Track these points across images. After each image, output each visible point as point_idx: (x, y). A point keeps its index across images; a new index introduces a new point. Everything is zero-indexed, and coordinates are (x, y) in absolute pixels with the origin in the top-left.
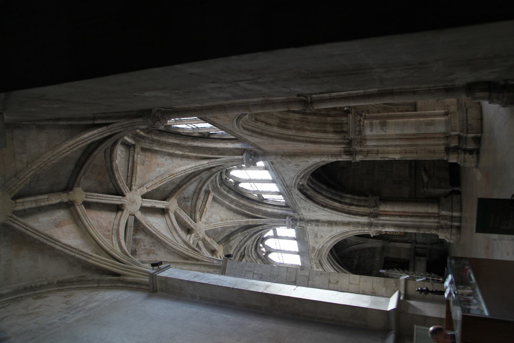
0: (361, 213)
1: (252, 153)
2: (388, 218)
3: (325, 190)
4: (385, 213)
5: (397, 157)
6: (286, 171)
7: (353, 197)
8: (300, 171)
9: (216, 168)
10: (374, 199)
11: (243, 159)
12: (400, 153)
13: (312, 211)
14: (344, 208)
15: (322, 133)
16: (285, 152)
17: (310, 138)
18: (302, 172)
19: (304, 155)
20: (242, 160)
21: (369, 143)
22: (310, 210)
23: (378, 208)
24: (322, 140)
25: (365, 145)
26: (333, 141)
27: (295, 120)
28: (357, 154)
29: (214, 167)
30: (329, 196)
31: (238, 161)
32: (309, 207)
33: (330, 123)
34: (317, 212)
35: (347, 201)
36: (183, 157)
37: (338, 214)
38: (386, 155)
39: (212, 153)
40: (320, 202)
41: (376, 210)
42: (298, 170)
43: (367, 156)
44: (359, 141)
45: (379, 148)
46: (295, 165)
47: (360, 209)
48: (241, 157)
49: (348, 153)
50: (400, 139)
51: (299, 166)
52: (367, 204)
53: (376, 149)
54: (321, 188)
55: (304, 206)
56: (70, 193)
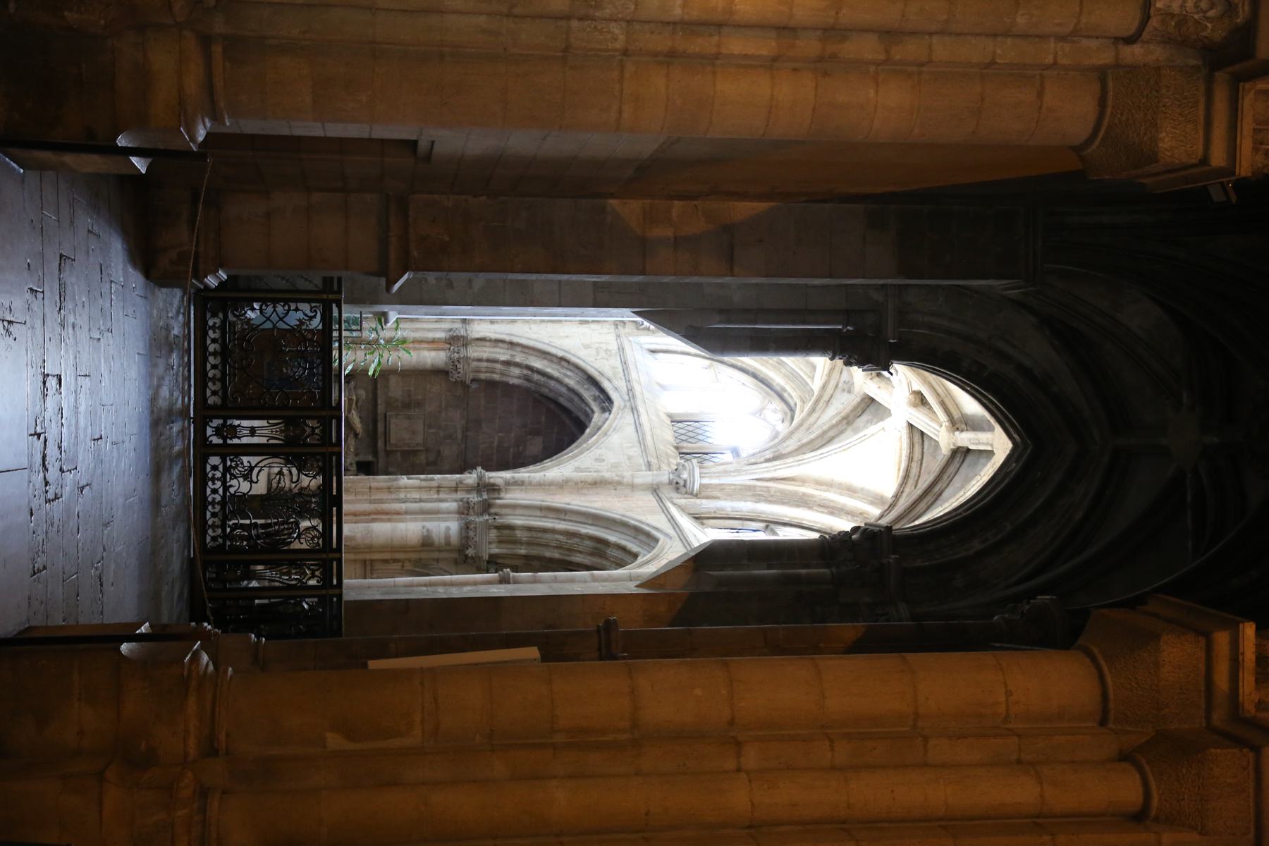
0: (488, 344)
1: (683, 490)
2: (431, 335)
3: (562, 397)
4: (435, 346)
5: (404, 480)
7: (505, 379)
9: (762, 459)
10: (460, 375)
12: (400, 488)
14: (524, 356)
15: (535, 526)
16: (615, 489)
18: (594, 444)
20: (703, 475)
21: (453, 506)
23: (450, 356)
24: (538, 513)
25: (461, 503)
26: (519, 511)
27: (581, 552)
28: (476, 485)
29: (768, 460)
30: (552, 383)
31: (714, 473)
32: (598, 358)
33: (522, 544)
34: (583, 345)
36: (829, 485)
37: (536, 340)
38: (424, 484)
39: (768, 491)
40: (572, 368)
41: (454, 352)
42: (601, 448)
43: (457, 484)
44: (471, 511)
45: (436, 496)
46: (604, 460)
47: (490, 352)
48: (705, 481)
49: (493, 488)
50: (398, 513)
51: (597, 460)
52: (475, 364)
53: (442, 496)
54: (571, 400)
55: (607, 359)
56: (952, 447)
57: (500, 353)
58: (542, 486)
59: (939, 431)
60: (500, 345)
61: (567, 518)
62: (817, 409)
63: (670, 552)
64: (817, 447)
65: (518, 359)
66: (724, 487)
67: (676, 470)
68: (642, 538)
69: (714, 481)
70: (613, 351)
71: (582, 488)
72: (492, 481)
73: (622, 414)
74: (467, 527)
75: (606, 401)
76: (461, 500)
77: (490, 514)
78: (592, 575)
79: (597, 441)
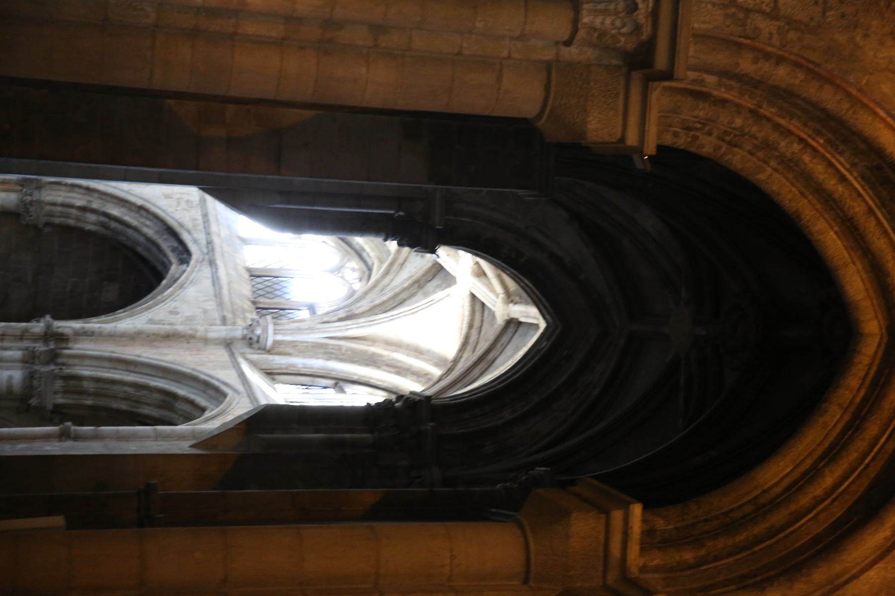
0: (63, 188)
6: (204, 301)
7: (80, 225)
8: (171, 301)
9: (335, 318)
11: (275, 334)
13: (172, 198)
16: (188, 343)
17: (127, 371)
19: (148, 336)
20: (276, 332)
21: (18, 354)
22: (178, 199)
23: (22, 197)
24: (107, 364)
25: (26, 352)
26: (87, 362)
30: (130, 232)
32: (179, 208)
35: (93, 218)
36: (397, 346)
40: (151, 217)
41: (27, 195)
42: (175, 301)
46: (177, 313)
48: (279, 338)
49: (61, 338)
51: (171, 312)
52: (49, 208)
54: (148, 250)
55: (187, 210)
57: (75, 198)
58: (112, 337)
59: (496, 302)
60: (77, 189)
61: (136, 370)
62: (392, 271)
63: (237, 407)
64: (388, 308)
65: (95, 206)
66: (297, 344)
67: (250, 325)
68: (211, 392)
69: (288, 338)
70: (194, 203)
71: (154, 341)
72: (60, 330)
73: (201, 266)
74: (31, 377)
75: (184, 254)
76: (27, 349)
77: (56, 364)
78: (155, 430)
79: (172, 294)
